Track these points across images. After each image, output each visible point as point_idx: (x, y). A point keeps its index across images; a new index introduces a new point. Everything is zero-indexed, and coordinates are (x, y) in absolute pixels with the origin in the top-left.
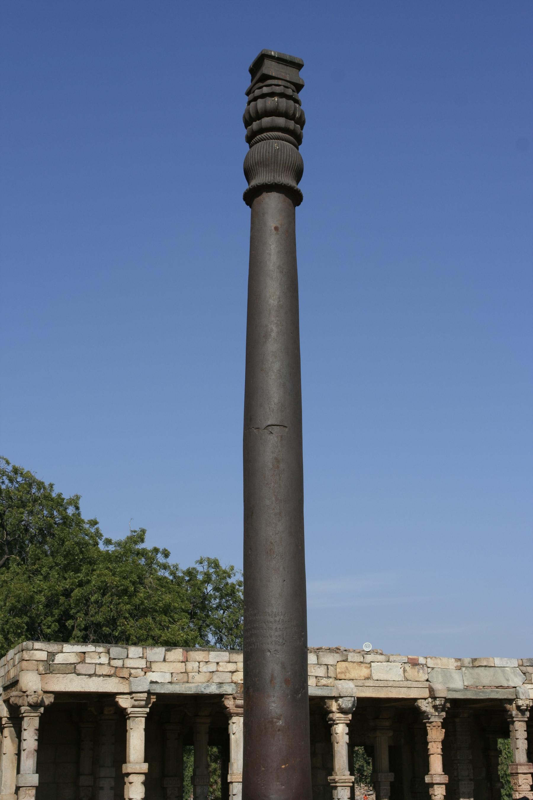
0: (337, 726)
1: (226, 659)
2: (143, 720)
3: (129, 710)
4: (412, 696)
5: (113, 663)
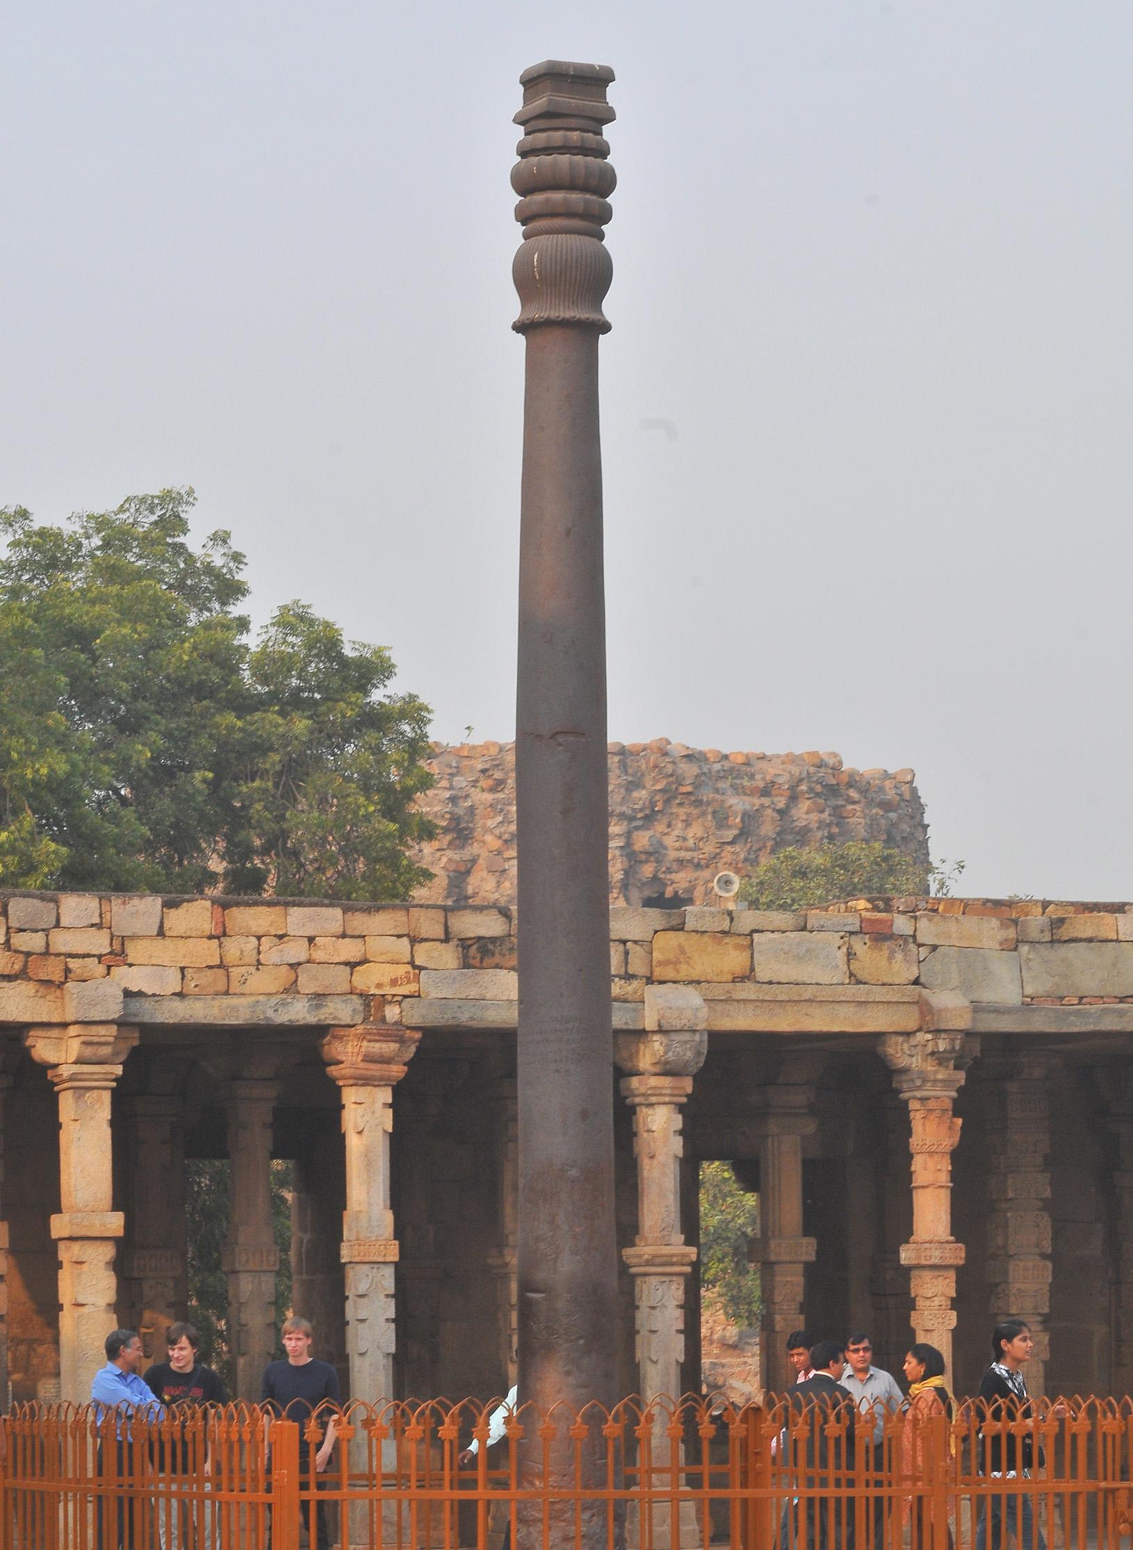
0: (650, 1112)
1: (337, 927)
2: (106, 1097)
3: (66, 1071)
4: (870, 1027)
5: (19, 941)
